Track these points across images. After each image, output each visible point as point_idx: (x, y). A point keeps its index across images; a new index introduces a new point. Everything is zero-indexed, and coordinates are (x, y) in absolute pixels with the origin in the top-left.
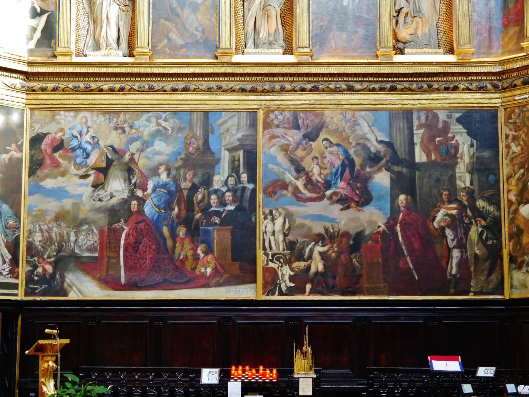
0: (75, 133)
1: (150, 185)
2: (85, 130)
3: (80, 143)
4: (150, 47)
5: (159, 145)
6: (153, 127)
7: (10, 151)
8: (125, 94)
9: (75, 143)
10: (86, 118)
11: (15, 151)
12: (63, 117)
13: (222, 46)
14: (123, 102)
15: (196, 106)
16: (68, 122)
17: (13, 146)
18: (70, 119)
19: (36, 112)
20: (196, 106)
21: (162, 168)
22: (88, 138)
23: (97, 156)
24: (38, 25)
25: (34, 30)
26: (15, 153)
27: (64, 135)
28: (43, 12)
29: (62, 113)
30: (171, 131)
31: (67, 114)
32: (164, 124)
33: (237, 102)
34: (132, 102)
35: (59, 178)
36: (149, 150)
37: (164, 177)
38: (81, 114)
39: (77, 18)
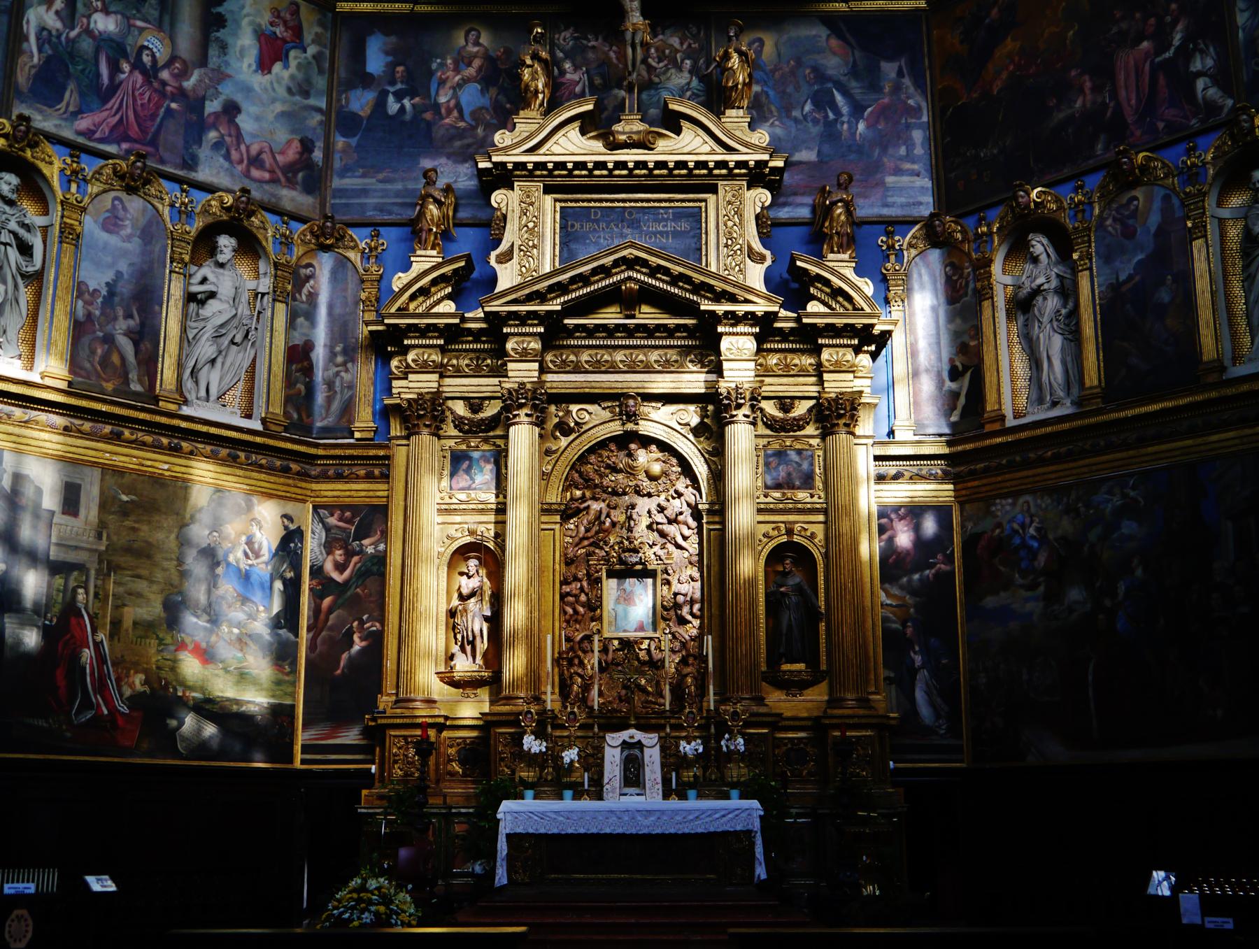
0: (1016, 526)
1: (1122, 588)
2: (1028, 520)
3: (1023, 539)
4: (1103, 384)
5: (1128, 527)
6: (1117, 501)
7: (934, 565)
8: (1075, 460)
9: (1017, 541)
10: (1028, 502)
11: (943, 563)
12: (999, 507)
13: (1205, 358)
14: (1075, 472)
15: (1178, 458)
16: (1007, 512)
17: (940, 557)
18: (1008, 508)
19: (967, 506)
20: (1178, 458)
21: (1136, 561)
22: (1032, 531)
23: (1045, 554)
24: (961, 388)
25: (954, 395)
26: (943, 566)
27: (1002, 532)
28: (966, 368)
29: (998, 501)
30: (1143, 503)
31: (1004, 502)
32: (1132, 494)
33: (1237, 441)
34: (1086, 470)
35: (1003, 594)
36: (1115, 535)
37: (1139, 572)
38: (1021, 500)
39: (1011, 366)
